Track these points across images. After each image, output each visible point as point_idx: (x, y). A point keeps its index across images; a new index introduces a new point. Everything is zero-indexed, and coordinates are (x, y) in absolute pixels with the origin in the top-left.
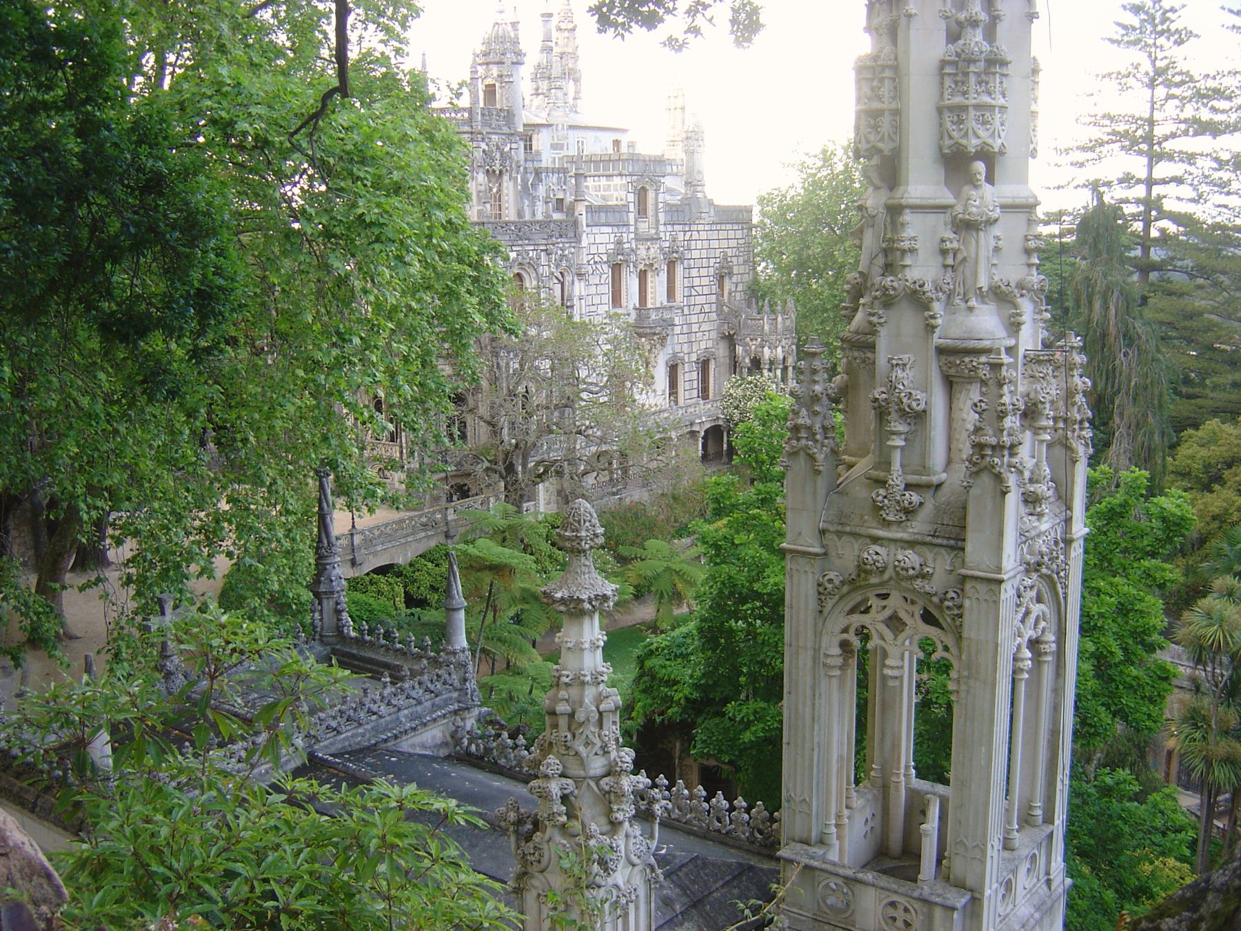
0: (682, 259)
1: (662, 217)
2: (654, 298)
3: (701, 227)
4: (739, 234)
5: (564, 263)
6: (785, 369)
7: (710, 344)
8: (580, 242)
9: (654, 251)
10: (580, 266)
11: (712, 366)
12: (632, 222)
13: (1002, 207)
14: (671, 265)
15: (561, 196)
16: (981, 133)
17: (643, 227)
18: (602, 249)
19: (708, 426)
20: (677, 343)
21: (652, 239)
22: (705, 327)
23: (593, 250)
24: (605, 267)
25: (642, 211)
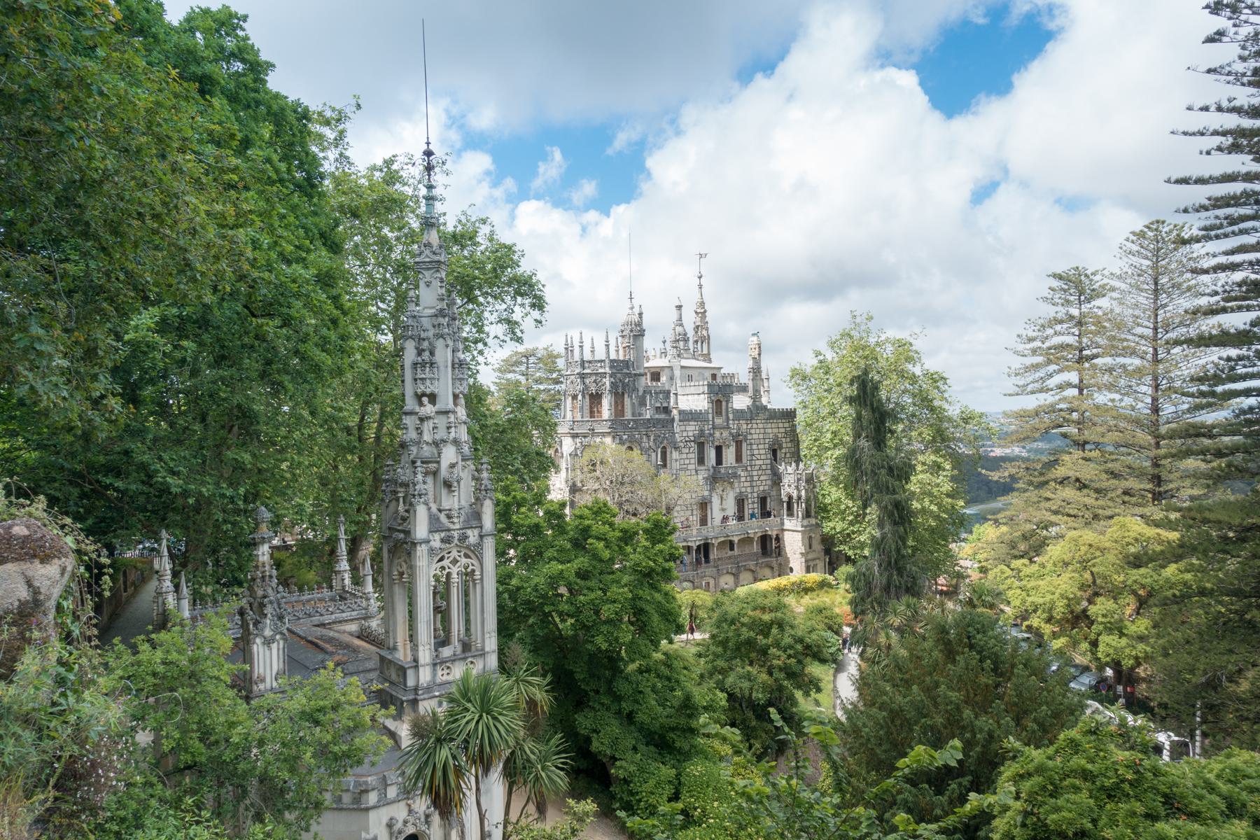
1: (731, 416)
4: (787, 425)
9: (726, 434)
14: (739, 445)
17: (719, 421)
18: (691, 434)
20: (742, 486)
25: (718, 412)
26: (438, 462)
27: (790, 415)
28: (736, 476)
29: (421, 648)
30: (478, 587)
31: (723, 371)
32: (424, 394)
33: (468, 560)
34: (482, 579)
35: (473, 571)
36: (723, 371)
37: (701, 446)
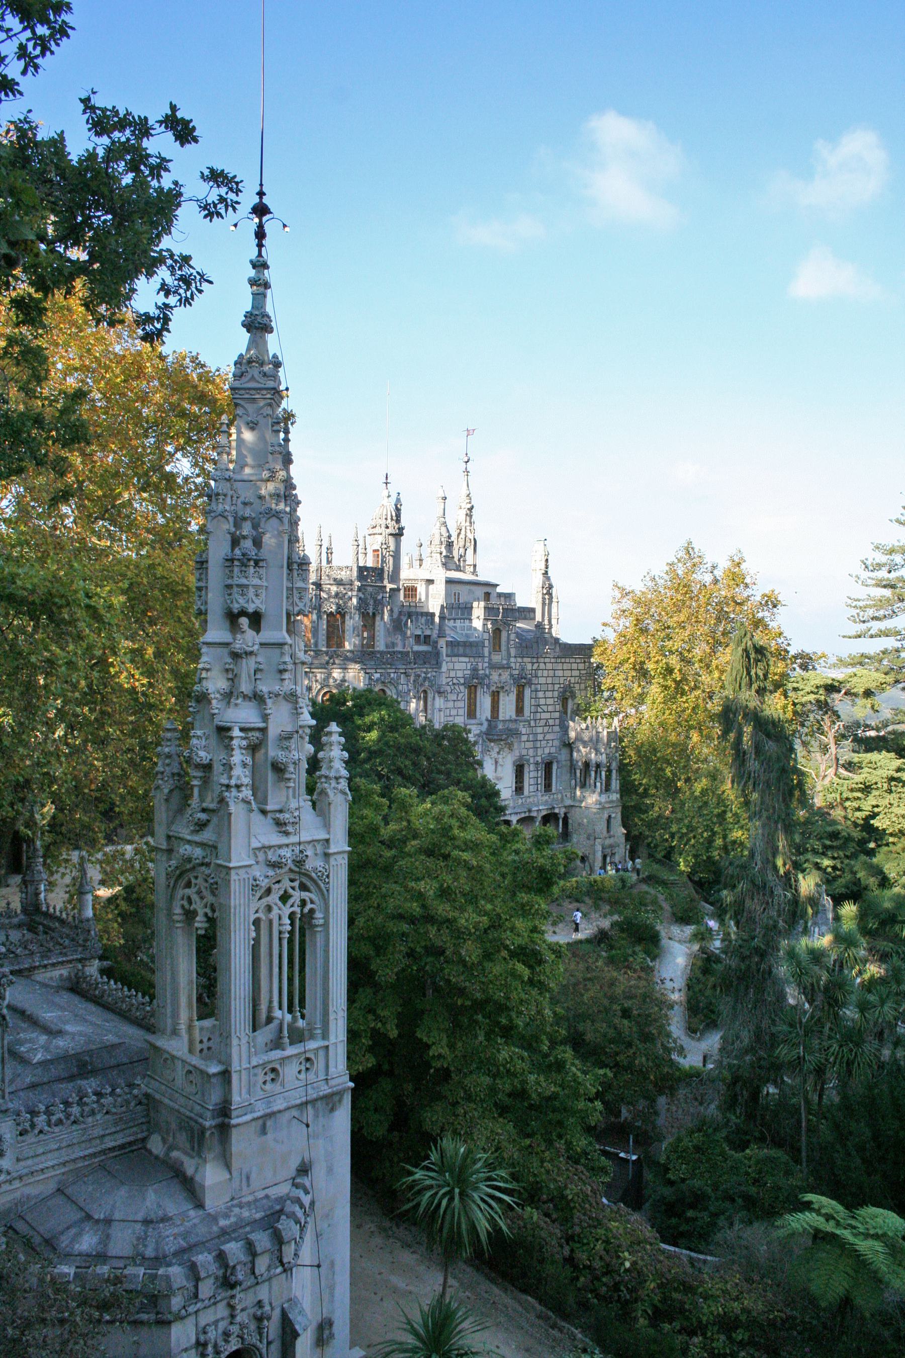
0: (530, 683)
1: (513, 652)
2: (505, 713)
3: (547, 660)
4: (581, 666)
5: (427, 684)
6: (609, 771)
7: (553, 750)
8: (440, 668)
9: (506, 676)
10: (440, 686)
11: (555, 767)
12: (486, 654)
13: (261, 644)
15: (428, 633)
16: (241, 601)
17: (496, 658)
18: (460, 674)
19: (544, 813)
21: (503, 667)
22: (548, 737)
23: (452, 674)
24: (462, 688)
26: (263, 730)
27: (584, 651)
28: (516, 733)
29: (235, 1042)
30: (319, 938)
31: (499, 590)
32: (243, 613)
33: (305, 895)
34: (326, 925)
35: (312, 911)
36: (499, 590)
37: (472, 690)
